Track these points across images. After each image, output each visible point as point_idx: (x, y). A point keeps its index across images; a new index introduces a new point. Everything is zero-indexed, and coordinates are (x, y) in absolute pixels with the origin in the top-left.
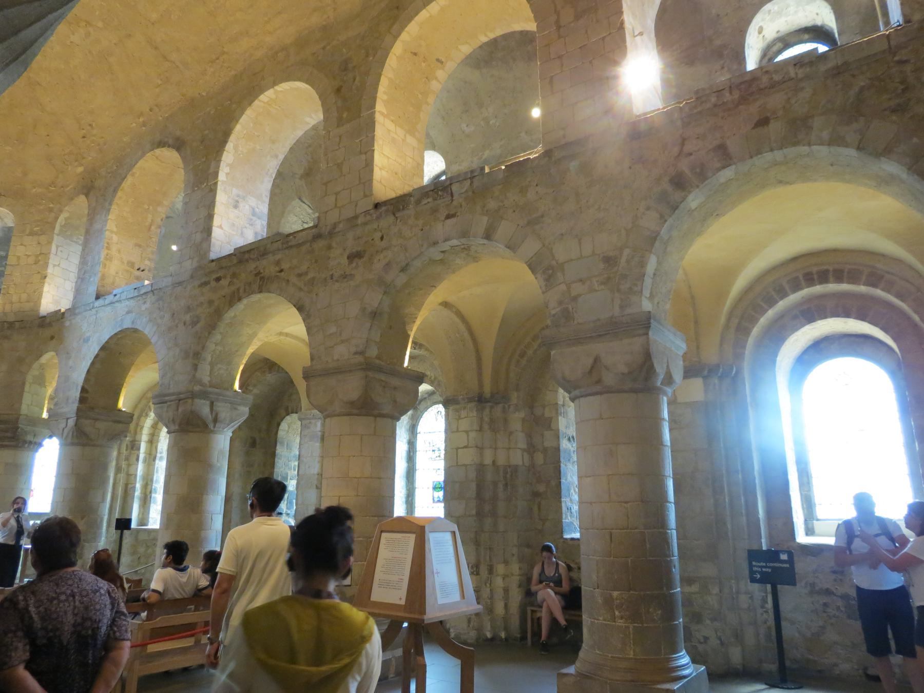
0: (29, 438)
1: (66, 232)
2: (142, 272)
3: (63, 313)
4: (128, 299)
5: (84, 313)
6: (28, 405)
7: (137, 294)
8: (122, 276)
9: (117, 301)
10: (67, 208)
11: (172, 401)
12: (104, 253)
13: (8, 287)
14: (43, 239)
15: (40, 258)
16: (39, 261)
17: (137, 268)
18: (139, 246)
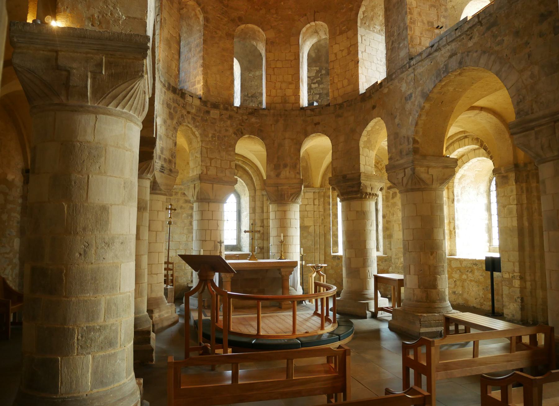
0: (369, 190)
1: (365, 24)
2: (441, 30)
3: (381, 83)
4: (448, 44)
5: (401, 76)
6: (364, 165)
7: (460, 34)
8: (426, 36)
9: (436, 51)
10: (363, 3)
11: (541, 125)
12: (409, 17)
13: (334, 79)
14: (350, 33)
15: (351, 49)
16: (351, 51)
17: (436, 27)
18: (434, 6)
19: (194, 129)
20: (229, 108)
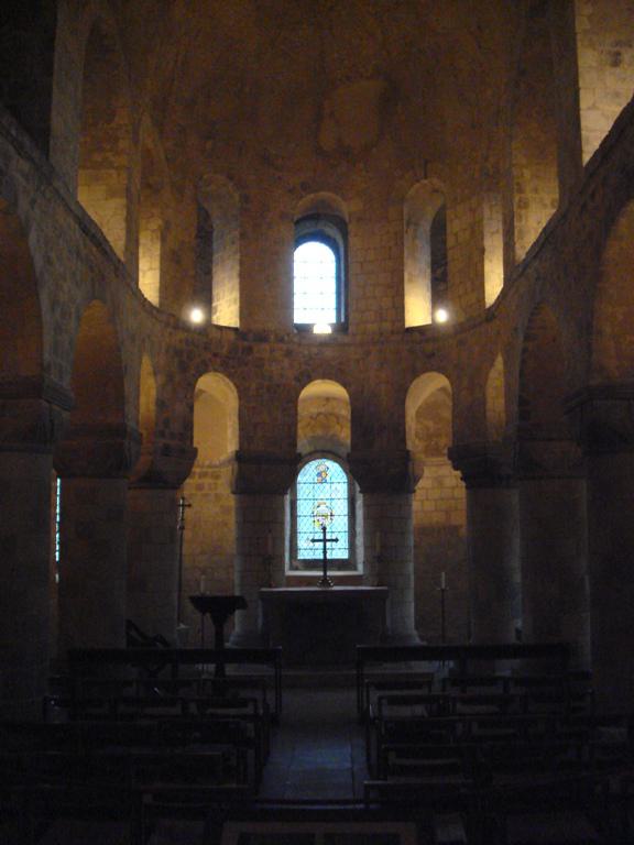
19: (227, 380)
20: (286, 338)
